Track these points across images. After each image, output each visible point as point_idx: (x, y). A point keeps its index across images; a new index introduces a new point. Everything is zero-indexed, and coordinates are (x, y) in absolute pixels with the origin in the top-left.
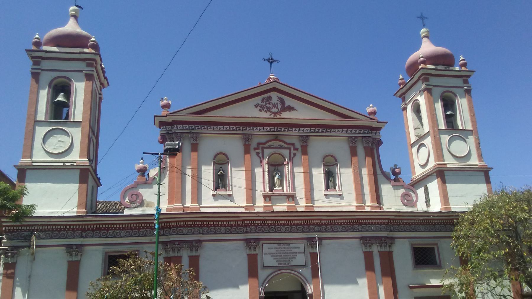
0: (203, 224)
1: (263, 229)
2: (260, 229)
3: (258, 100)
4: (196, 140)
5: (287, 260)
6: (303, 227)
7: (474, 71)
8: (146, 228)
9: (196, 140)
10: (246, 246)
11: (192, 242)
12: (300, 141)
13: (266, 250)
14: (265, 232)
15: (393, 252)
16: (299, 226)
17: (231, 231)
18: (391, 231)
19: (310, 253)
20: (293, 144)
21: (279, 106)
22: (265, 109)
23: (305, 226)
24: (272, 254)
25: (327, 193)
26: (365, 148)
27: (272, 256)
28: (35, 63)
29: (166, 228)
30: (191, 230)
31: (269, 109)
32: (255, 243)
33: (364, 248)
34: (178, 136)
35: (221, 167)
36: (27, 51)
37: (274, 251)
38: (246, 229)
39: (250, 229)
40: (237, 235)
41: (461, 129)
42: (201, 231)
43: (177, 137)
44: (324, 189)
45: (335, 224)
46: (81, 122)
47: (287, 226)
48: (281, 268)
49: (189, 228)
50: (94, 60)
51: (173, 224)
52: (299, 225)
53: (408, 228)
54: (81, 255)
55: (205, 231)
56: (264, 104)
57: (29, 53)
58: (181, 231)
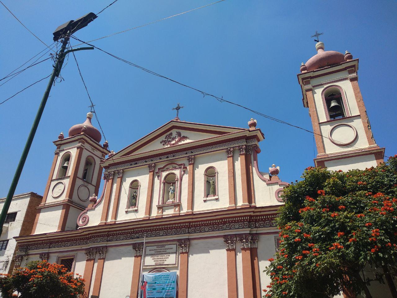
3: (163, 138)
5: (162, 259)
6: (177, 230)
13: (148, 252)
15: (257, 248)
16: (173, 230)
18: (256, 227)
22: (167, 143)
23: (178, 229)
25: (205, 199)
28: (58, 148)
36: (54, 142)
37: (153, 252)
44: (203, 196)
45: (202, 226)
46: (70, 176)
47: (164, 231)
50: (82, 138)
52: (174, 229)
54: (48, 260)
57: (55, 143)
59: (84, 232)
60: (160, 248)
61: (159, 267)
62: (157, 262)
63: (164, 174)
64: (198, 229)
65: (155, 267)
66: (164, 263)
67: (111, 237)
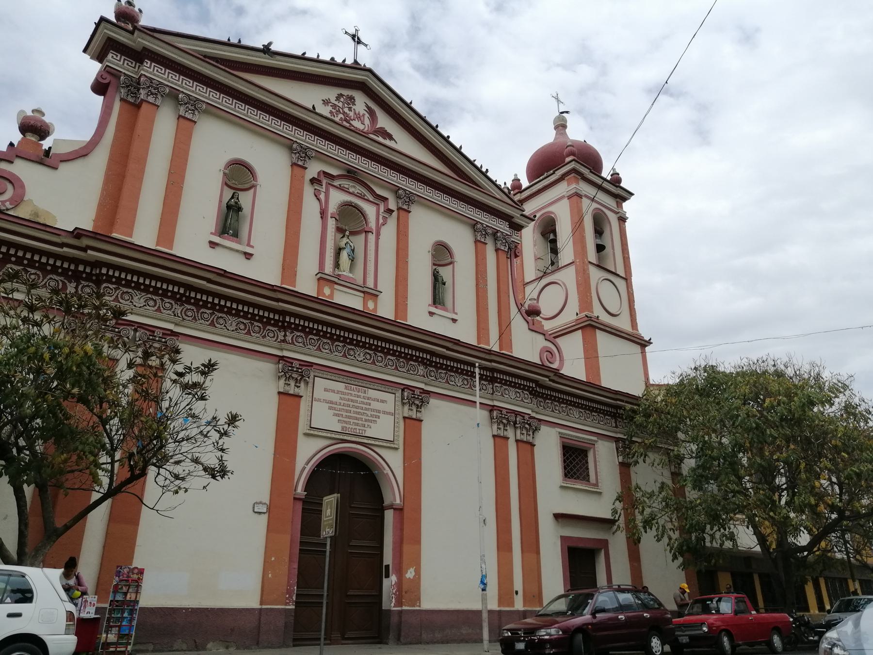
0: (187, 294)
1: (320, 344)
2: (313, 341)
3: (331, 93)
4: (193, 114)
5: (360, 422)
7: (632, 194)
8: (28, 265)
9: (193, 114)
10: (282, 371)
11: (154, 332)
12: (398, 197)
13: (319, 393)
14: (323, 350)
15: (535, 445)
17: (249, 329)
19: (404, 418)
20: (385, 199)
21: (367, 121)
23: (401, 360)
24: (331, 402)
26: (497, 250)
27: (330, 408)
29: (86, 280)
30: (155, 301)
31: (348, 118)
32: (301, 369)
33: (495, 426)
34: (152, 87)
35: (234, 193)
37: (335, 398)
38: (283, 334)
39: (292, 335)
40: (261, 340)
41: (614, 271)
42: (179, 312)
43: (149, 87)
45: (451, 371)
47: (368, 351)
48: (345, 438)
49: (149, 296)
51: (111, 273)
52: (393, 355)
53: (557, 408)
55: (189, 314)
56: (340, 104)
58: (127, 297)
59: (89, 252)
60: (353, 393)
61: (354, 439)
62: (348, 426)
63: (336, 198)
64: (442, 375)
65: (341, 437)
66: (365, 431)
67: (189, 307)
